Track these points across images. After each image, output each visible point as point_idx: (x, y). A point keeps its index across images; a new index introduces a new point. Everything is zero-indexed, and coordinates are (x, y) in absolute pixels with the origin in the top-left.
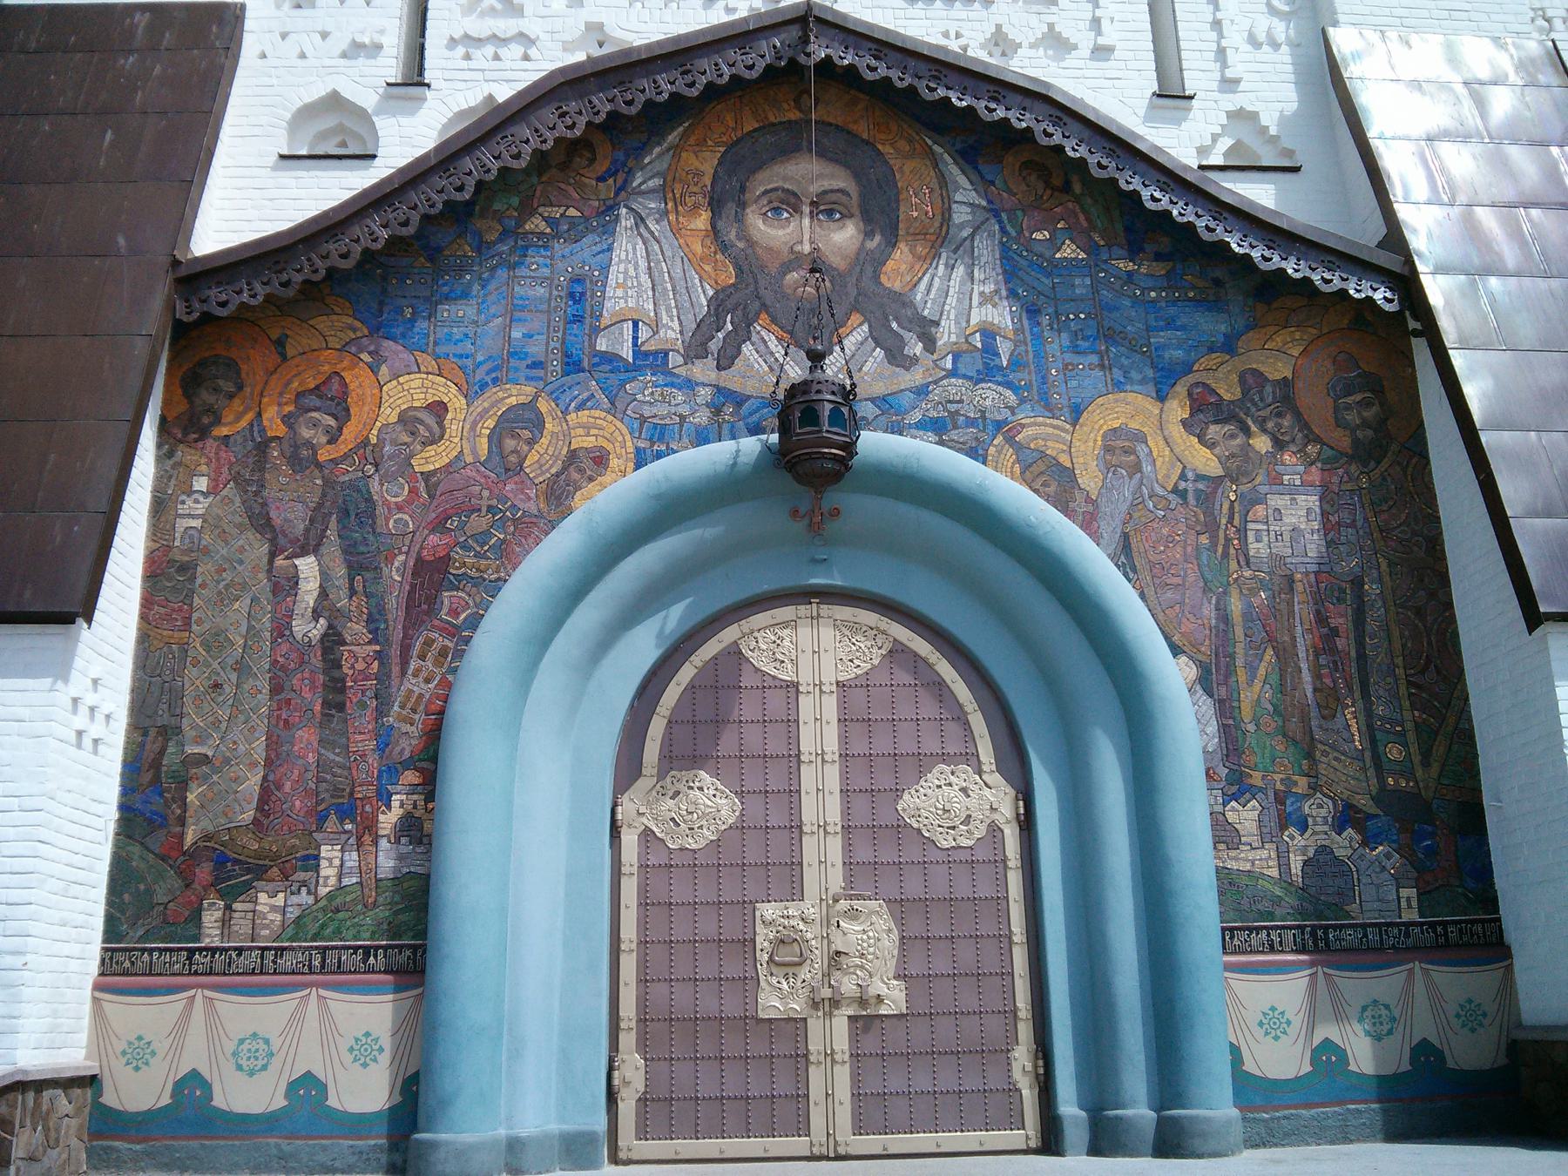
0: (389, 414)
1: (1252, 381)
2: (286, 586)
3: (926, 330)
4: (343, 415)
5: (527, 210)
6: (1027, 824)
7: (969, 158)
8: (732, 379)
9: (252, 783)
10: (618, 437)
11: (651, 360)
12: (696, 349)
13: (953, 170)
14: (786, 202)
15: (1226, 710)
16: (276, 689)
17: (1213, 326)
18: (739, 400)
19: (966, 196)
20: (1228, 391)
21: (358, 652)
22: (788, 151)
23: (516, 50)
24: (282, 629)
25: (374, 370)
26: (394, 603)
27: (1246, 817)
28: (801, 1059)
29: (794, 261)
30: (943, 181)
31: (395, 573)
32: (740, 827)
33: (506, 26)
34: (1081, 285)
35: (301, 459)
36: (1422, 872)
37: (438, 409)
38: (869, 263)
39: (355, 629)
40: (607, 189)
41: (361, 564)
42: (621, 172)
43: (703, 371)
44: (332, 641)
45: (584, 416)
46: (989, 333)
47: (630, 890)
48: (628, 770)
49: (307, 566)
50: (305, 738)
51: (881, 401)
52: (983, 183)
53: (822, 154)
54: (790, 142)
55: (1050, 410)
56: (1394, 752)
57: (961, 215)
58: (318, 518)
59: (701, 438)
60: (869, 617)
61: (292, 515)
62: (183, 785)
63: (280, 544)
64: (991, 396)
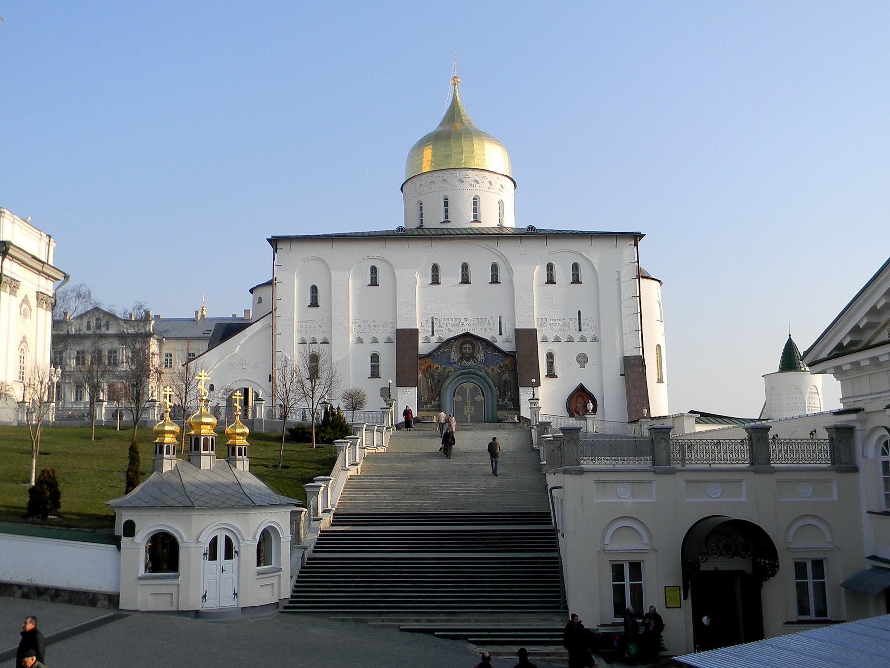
3: (477, 360)
4: (431, 367)
10: (453, 370)
11: (455, 363)
12: (458, 362)
16: (428, 390)
21: (434, 387)
22: (465, 344)
23: (442, 332)
27: (500, 400)
29: (467, 354)
35: (428, 371)
37: (438, 367)
38: (473, 353)
39: (433, 385)
44: (432, 386)
46: (482, 360)
49: (429, 380)
53: (469, 344)
54: (465, 342)
61: (428, 376)
64: (482, 365)
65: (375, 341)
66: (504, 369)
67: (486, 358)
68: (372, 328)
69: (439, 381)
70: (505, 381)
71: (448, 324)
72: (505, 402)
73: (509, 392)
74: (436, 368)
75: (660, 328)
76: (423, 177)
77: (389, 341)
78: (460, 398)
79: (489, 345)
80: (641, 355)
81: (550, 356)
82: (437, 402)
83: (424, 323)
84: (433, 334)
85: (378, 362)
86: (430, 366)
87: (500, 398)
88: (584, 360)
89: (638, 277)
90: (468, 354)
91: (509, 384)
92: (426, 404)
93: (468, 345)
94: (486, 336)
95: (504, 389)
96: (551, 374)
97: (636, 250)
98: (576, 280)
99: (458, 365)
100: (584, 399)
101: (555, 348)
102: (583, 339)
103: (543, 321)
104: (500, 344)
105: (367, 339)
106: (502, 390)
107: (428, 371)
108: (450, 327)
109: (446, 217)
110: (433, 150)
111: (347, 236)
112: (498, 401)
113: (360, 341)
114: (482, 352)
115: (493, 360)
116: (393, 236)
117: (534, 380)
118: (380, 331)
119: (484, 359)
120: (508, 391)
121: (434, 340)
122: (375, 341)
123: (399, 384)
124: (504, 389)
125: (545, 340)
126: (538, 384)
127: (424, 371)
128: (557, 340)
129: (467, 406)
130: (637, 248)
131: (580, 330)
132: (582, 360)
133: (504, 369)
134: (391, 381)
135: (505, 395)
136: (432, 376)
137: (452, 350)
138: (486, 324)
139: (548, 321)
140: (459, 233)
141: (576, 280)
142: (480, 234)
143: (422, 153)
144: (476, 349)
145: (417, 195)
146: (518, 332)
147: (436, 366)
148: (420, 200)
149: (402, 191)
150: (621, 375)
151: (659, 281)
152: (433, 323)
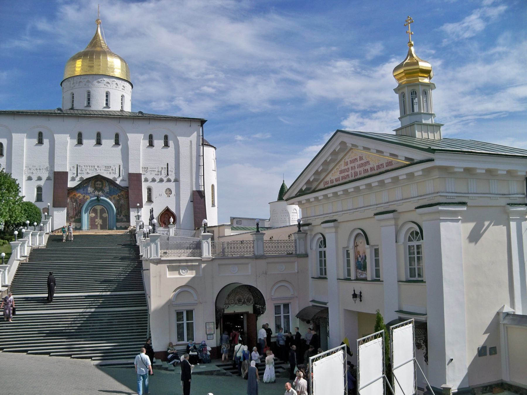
0: (78, 196)
1: (121, 194)
2: (73, 204)
3: (105, 191)
4: (75, 196)
5: (84, 184)
6: (108, 216)
7: (107, 181)
8: (95, 194)
9: (72, 214)
11: (91, 193)
12: (93, 192)
13: (107, 182)
14: (98, 184)
15: (118, 211)
16: (73, 209)
17: (119, 191)
18: (95, 195)
19: (107, 184)
20: (120, 195)
21: (77, 208)
24: (73, 207)
25: (77, 193)
26: (78, 205)
27: (118, 216)
28: (97, 226)
29: (98, 187)
30: (106, 183)
31: (78, 204)
32: (95, 216)
33: (82, 172)
34: (113, 189)
35: (73, 198)
36: (126, 218)
37: (80, 196)
38: (102, 187)
39: (77, 207)
40: (88, 183)
41: (77, 203)
42: (89, 182)
43: (93, 193)
44: (76, 207)
45: (87, 196)
46: (108, 191)
47: (90, 219)
48: (90, 213)
49: (74, 204)
50: (75, 212)
51: (102, 195)
52: (108, 183)
53: (100, 181)
54: (98, 181)
55: (111, 196)
56: (126, 213)
57: (107, 185)
58: (75, 201)
59: (93, 197)
60: (101, 206)
61: (73, 201)
62: (69, 214)
63: (73, 203)
64: (108, 195)
65: (39, 179)
66: (121, 197)
67: (110, 191)
68: (39, 171)
69: (80, 204)
70: (122, 205)
71: (87, 169)
72: (121, 217)
73: (124, 211)
74: (79, 196)
75: (214, 174)
76: (75, 78)
77: (48, 179)
78: (93, 215)
79: (111, 182)
80: (203, 190)
81: (149, 190)
82: (79, 217)
83: (72, 169)
84: (77, 175)
85: (41, 191)
86: (75, 195)
87: (118, 215)
88: (170, 192)
89: (203, 145)
90: (99, 188)
91: (124, 206)
92: (72, 218)
93: (99, 182)
94: (111, 177)
95: (121, 210)
96: (150, 200)
97: (201, 129)
98: (166, 145)
99: (93, 194)
100: (168, 215)
101: (153, 185)
102: (169, 180)
103: (146, 169)
104: (118, 182)
105: (35, 178)
106: (119, 210)
107: (73, 198)
108: (88, 171)
109: (89, 103)
110: (82, 62)
111: (24, 112)
112: (117, 216)
113: (30, 179)
114: (108, 187)
115: (114, 192)
116: (54, 113)
117: (138, 205)
118: (44, 172)
119: (109, 191)
120: (123, 210)
121: (78, 179)
122: (39, 179)
123: (54, 206)
124: (121, 210)
125: (146, 180)
126: (141, 206)
127: (71, 199)
128: (154, 180)
129: (97, 219)
130: (202, 128)
131: (168, 174)
132: (169, 191)
133: (121, 197)
134: (49, 204)
135: (121, 213)
136: (76, 201)
137: (89, 185)
138: (110, 170)
139: (149, 169)
140: (96, 114)
141: (166, 145)
142: (109, 115)
143: (75, 64)
144: (104, 185)
145: (71, 89)
146: (130, 175)
147: (79, 195)
148: (72, 93)
149: (61, 85)
150: (191, 202)
151: (215, 148)
152: (77, 168)
